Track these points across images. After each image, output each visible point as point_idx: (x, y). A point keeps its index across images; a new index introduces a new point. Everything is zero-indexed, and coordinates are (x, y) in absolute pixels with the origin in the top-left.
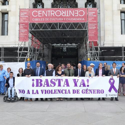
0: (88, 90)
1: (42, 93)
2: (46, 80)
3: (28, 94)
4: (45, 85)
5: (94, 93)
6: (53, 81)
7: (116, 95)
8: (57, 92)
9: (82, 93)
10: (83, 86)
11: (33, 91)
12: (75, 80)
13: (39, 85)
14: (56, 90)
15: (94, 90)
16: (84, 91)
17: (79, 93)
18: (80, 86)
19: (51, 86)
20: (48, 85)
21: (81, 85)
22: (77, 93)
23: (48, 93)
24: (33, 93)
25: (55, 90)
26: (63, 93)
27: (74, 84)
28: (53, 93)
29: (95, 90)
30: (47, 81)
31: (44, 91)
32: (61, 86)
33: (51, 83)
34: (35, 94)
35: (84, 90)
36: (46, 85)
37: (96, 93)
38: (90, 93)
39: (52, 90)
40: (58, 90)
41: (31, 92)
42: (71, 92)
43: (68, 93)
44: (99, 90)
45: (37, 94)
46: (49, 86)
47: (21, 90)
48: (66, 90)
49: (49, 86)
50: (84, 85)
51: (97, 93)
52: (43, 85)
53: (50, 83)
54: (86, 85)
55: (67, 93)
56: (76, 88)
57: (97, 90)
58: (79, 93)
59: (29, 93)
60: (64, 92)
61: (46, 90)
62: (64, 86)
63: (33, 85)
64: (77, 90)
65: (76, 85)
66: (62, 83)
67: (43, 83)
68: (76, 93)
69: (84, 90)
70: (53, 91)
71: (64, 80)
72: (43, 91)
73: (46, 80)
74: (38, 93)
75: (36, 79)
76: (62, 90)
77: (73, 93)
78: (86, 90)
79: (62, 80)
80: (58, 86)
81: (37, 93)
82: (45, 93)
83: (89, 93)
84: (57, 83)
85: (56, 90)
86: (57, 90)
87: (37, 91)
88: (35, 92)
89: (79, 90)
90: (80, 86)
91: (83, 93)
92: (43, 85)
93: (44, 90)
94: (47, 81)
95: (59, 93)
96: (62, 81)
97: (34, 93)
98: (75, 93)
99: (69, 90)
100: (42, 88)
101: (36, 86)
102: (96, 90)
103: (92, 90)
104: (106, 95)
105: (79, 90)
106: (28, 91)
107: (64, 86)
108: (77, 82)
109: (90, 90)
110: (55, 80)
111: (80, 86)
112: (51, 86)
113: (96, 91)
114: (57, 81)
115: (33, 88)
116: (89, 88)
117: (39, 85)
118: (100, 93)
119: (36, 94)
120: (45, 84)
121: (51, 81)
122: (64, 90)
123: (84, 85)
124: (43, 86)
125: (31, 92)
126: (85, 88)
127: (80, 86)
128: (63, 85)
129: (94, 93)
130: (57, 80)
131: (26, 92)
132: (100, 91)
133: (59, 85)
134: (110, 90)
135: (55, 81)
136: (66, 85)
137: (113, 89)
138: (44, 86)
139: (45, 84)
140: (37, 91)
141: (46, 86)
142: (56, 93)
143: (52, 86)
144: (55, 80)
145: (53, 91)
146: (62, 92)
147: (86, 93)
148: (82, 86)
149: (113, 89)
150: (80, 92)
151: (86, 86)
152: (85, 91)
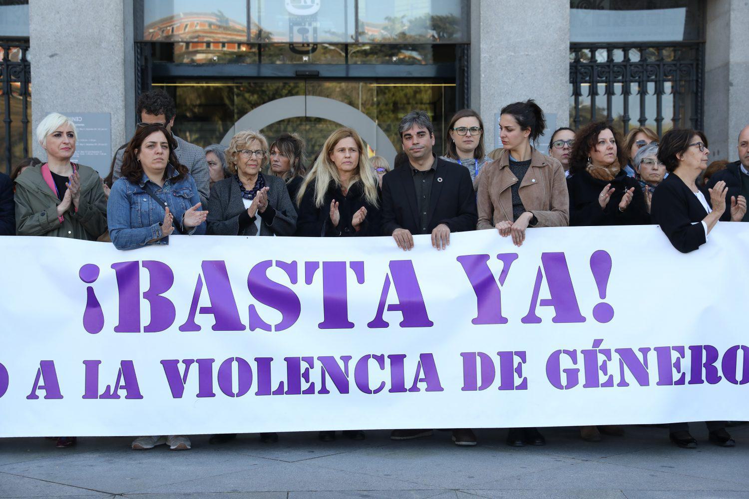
0: (607, 353)
1: (177, 389)
2: (206, 265)
3: (42, 401)
4: (199, 319)
6: (278, 276)
9: (554, 379)
11: (92, 368)
13: (145, 316)
14: (310, 361)
16: (565, 362)
17: (524, 386)
18: (531, 318)
19: (256, 322)
21: (540, 311)
22: (507, 385)
23: (227, 391)
24: (91, 391)
25: (293, 364)
26: (373, 385)
28: (280, 391)
31: (195, 368)
34: (107, 395)
35: (573, 355)
36: (209, 320)
38: (623, 383)
39: (264, 364)
40: (328, 363)
43: (414, 389)
44: (712, 352)
45: (124, 402)
46: (242, 328)
48: (397, 360)
49: (242, 328)
51: (696, 379)
52: (181, 317)
53: (243, 300)
55: (408, 384)
58: (524, 386)
59: (53, 392)
60: (378, 375)
61: (205, 366)
62: (378, 323)
64: (506, 357)
69: (573, 355)
70: (279, 374)
72: (181, 367)
74: (134, 393)
76: (368, 357)
77: (469, 385)
78: (590, 356)
81: (123, 393)
82: (205, 391)
85: (304, 366)
86: (318, 365)
87: (127, 369)
88: (107, 377)
89: (522, 355)
90: (525, 320)
91: (564, 380)
92: (181, 317)
93: (188, 363)
96: (361, 280)
97: (101, 390)
98: (488, 381)
99: (427, 360)
101: (117, 329)
103: (645, 351)
105: (522, 355)
106: (47, 369)
107: (378, 323)
109: (626, 355)
112: (256, 322)
114: (309, 280)
117: (145, 317)
118: (713, 379)
119: (116, 396)
120: (204, 311)
122: (380, 359)
124: (183, 328)
127: (531, 318)
132: (718, 364)
135: (294, 280)
138: (190, 326)
139: (204, 311)
140: (127, 369)
141: (206, 321)
142: (304, 386)
143: (267, 328)
144: (290, 269)
145: (279, 374)
147: (592, 382)
148: (547, 313)
151: (583, 320)
152: (581, 365)
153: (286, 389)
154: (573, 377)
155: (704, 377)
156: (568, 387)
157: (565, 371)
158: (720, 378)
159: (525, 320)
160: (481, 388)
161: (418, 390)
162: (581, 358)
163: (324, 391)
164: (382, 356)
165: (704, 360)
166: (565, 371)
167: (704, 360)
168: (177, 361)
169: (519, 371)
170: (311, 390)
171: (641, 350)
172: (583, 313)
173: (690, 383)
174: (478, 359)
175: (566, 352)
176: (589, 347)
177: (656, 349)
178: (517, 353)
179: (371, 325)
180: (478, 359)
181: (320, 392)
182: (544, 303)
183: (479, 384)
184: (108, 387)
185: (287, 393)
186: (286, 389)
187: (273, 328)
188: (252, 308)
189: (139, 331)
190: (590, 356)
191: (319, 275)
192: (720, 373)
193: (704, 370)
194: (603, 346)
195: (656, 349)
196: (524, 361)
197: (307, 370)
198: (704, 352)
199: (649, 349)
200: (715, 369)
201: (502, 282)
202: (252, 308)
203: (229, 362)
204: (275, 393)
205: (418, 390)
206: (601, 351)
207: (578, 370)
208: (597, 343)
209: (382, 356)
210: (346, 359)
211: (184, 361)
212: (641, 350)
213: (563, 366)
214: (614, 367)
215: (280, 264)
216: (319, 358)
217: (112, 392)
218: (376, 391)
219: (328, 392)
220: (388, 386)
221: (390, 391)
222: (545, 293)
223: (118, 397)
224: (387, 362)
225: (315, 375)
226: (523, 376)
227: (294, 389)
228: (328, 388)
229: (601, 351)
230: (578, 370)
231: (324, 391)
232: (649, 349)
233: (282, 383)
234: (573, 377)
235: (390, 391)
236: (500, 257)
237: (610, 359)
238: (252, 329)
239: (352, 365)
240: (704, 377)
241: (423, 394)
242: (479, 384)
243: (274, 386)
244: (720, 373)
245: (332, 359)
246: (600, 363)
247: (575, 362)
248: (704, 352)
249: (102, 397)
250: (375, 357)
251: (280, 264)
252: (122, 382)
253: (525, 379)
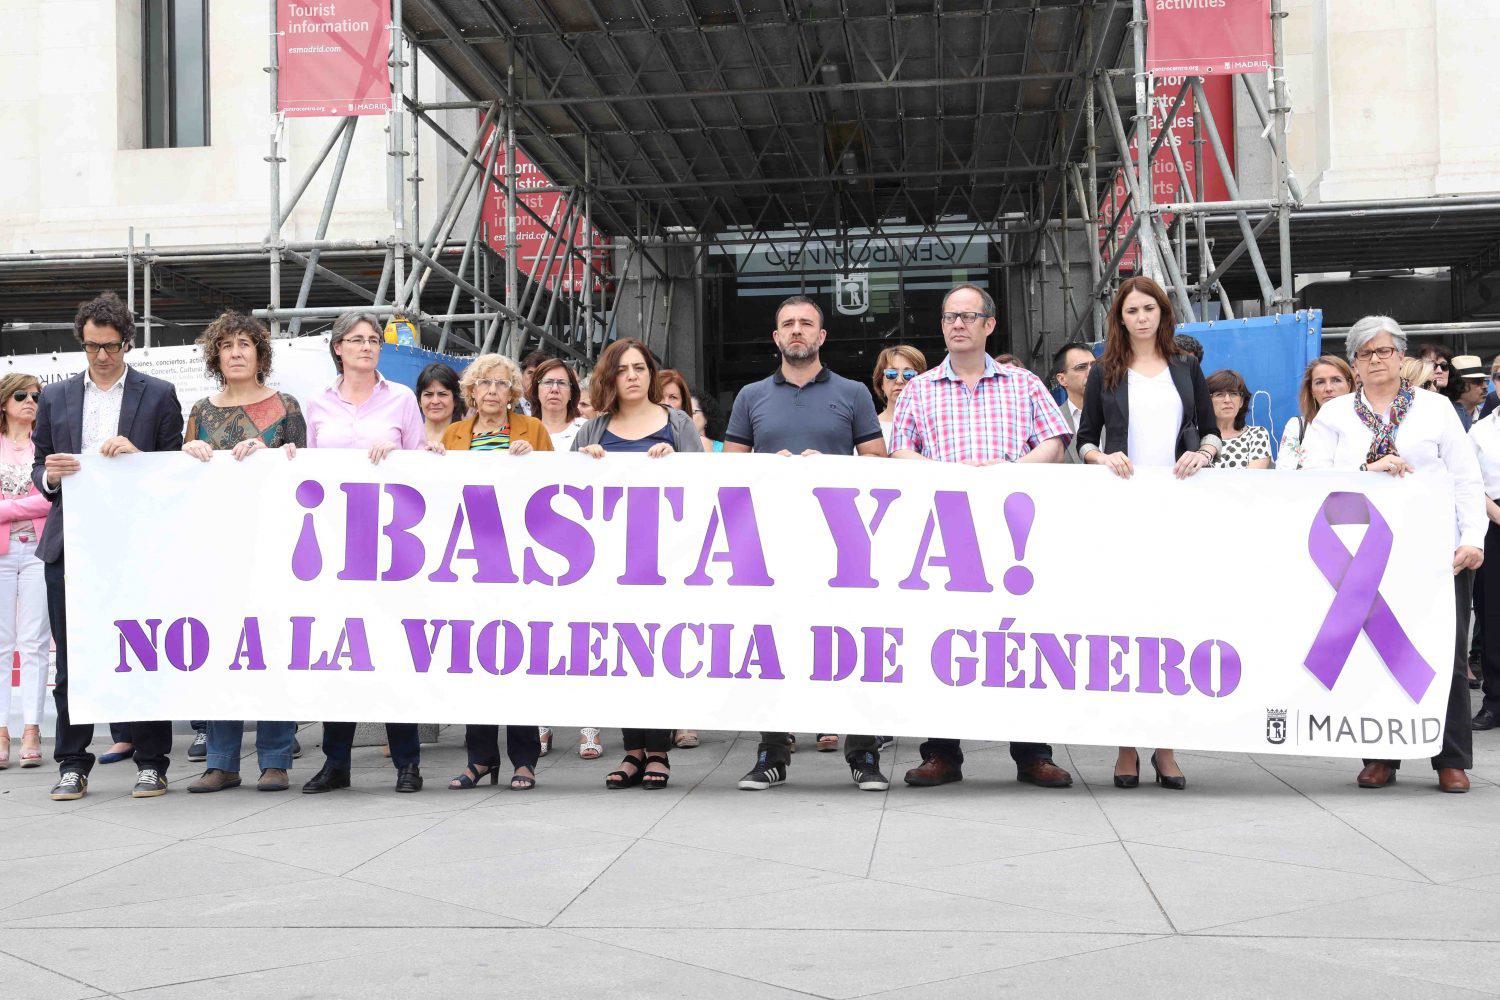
0: (1020, 639)
1: (422, 662)
2: (471, 493)
5: (1098, 682)
7: (1406, 732)
8: (609, 649)
10: (949, 587)
11: (302, 628)
12: (836, 505)
13: (384, 560)
14: (602, 628)
15: (1099, 644)
16: (959, 648)
17: (897, 677)
18: (914, 582)
19: (534, 572)
20: (494, 568)
21: (928, 573)
22: (873, 674)
23: (488, 663)
24: (299, 660)
25: (579, 630)
26: (686, 666)
27: (826, 555)
28: (559, 670)
29: (1123, 641)
30: (481, 506)
31: (446, 633)
32: (661, 581)
33: (529, 541)
34: (322, 664)
35: (971, 637)
37: (1124, 686)
39: (541, 630)
40: (628, 632)
41: (277, 645)
42: (795, 653)
43: (744, 674)
44: (1175, 649)
47: (154, 624)
48: (722, 633)
49: (514, 579)
50: (967, 575)
51: (1148, 685)
52: (433, 561)
53: (517, 537)
54: (995, 571)
55: (735, 666)
56: (853, 610)
57: (1148, 646)
58: (897, 677)
60: (695, 652)
61: (461, 630)
62: (699, 578)
63: (306, 563)
64: (873, 635)
65: (853, 571)
66: (678, 545)
67: (432, 532)
68: (860, 668)
69: (971, 637)
70: (560, 646)
71: (702, 504)
72: (429, 630)
73: (471, 493)
74: (362, 660)
75: (345, 487)
77: (821, 672)
78: (995, 641)
79: (676, 495)
80: (622, 580)
81: (345, 662)
82: (459, 664)
83: (1030, 678)
84: (610, 537)
85: (594, 634)
86: (613, 634)
87: (355, 630)
88: (323, 640)
89: (897, 634)
90: (905, 584)
91: (955, 674)
92: (433, 561)
93: (438, 624)
94: (481, 506)
95: (629, 663)
96: (678, 515)
97: (314, 657)
98: (846, 668)
99: (763, 637)
100: (421, 597)
101: (342, 576)
102: (1134, 647)
103: (1073, 639)
104: (1277, 720)
105: (897, 634)
107: (699, 578)
108: (875, 525)
110: (583, 497)
111: (904, 584)
112: (534, 572)
113: (1132, 664)
114: (608, 514)
115: (306, 598)
116: (1032, 614)
117: (384, 560)
118: (1177, 687)
119: (335, 666)
121: (539, 513)
122: (698, 630)
123: (967, 575)
124: (434, 577)
125: (277, 645)
126: (981, 611)
127: (914, 582)
128: (690, 568)
129: (1098, 682)
130: (612, 495)
131: (224, 642)
132: (1185, 666)
133: (642, 569)
134: (1326, 662)
135: (588, 514)
136: (720, 571)
137: (1363, 650)
138: (444, 574)
140: (355, 630)
141: (466, 568)
142: (594, 663)
143: (547, 580)
144: (583, 497)
145: (560, 646)
146: (673, 664)
147: (995, 678)
148: (938, 576)
149: (1363, 650)
150: (914, 655)
151: (989, 588)
152: (981, 652)
153: (568, 667)
154: (968, 667)
155: (1162, 683)
156: (963, 682)
157: (957, 659)
158: (1189, 687)
159: (905, 584)
160: (838, 678)
161: (748, 676)
162: (981, 643)
163: (620, 671)
164: (702, 625)
165: (1162, 659)
166: (958, 659)
167: (1162, 659)
168: (423, 622)
169: (891, 656)
170: (601, 671)
171: (1067, 637)
172: (990, 579)
173: (1138, 690)
174: (835, 636)
175: (961, 633)
176: (996, 629)
177: (1089, 638)
178: (890, 631)
179: (689, 581)
180: (835, 636)
181: (614, 674)
182: (935, 561)
183: (835, 671)
184: (325, 654)
185: (569, 673)
186: (568, 667)
187: (555, 581)
188: (529, 553)
189: (373, 577)
190: (995, 641)
191: (621, 507)
192: (1188, 680)
193: (1162, 675)
194: (1014, 629)
195: (1089, 638)
196: (900, 641)
197: (598, 641)
198: (1162, 650)
199: (1078, 637)
200: (1181, 674)
201: (873, 534)
202: (529, 553)
203: (493, 626)
204: (554, 672)
205: (748, 676)
206: (1013, 636)
207: (975, 661)
208: (1007, 623)
209: (702, 625)
210: (652, 628)
211: (433, 622)
212: (1067, 637)
213: (954, 655)
214: (1027, 659)
215: (569, 490)
216: (616, 626)
217: (329, 661)
218: (691, 675)
219: (624, 674)
220: (707, 667)
221: (710, 675)
222: (937, 548)
223: (338, 668)
224: (708, 634)
225: (609, 649)
226: (897, 663)
227: (579, 667)
228: (625, 667)
229: (1011, 636)
230: (975, 661)
231: (620, 671)
232: (1078, 637)
233: (563, 659)
234: (968, 667)
235: (710, 675)
236: (875, 493)
237: (1022, 647)
238: (527, 581)
239: (660, 636)
240: (1162, 683)
241: (756, 682)
242: (835, 671)
243: (553, 663)
244: (1188, 680)
245: (633, 626)
246: (1008, 652)
247: (973, 648)
248: (1162, 650)
249: (314, 667)
250: (691, 626)
251: (570, 490)
252: (346, 648)
253: (900, 668)
